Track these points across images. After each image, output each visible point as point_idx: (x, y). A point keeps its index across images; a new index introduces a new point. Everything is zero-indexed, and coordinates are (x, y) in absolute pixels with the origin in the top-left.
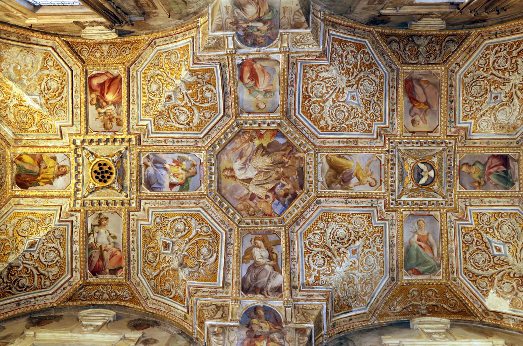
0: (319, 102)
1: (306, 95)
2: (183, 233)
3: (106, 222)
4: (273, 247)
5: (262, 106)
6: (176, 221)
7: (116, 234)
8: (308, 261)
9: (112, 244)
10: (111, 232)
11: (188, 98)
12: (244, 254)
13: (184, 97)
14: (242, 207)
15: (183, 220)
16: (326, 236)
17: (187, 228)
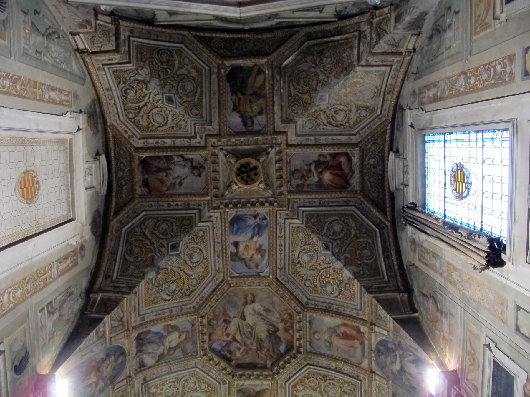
0: (320, 387)
1: (326, 377)
2: (189, 262)
3: (196, 174)
4: (180, 349)
5: (317, 336)
6: (201, 253)
7: (184, 185)
8: (170, 382)
9: (173, 181)
10: (186, 180)
11: (325, 268)
13: (326, 263)
14: (217, 314)
16: (193, 392)
17: (195, 265)
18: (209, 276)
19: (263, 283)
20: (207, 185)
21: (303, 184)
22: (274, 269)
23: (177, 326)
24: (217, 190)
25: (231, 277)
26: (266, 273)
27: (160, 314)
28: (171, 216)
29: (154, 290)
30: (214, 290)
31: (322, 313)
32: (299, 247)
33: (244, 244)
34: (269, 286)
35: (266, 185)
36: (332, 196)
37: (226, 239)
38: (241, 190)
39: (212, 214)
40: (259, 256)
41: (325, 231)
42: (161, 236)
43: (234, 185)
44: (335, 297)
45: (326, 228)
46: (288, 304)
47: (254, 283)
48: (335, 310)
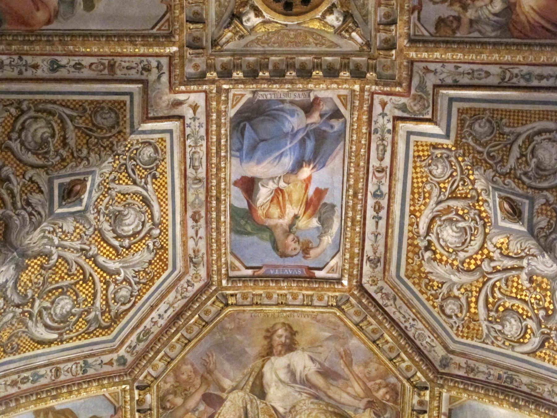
2: (110, 235)
6: (145, 208)
11: (505, 270)
12: (58, 408)
13: (508, 256)
14: (184, 377)
15: (148, 226)
17: (126, 243)
18: (164, 276)
19: (320, 299)
20: (169, 9)
21: (458, 19)
22: (356, 261)
23: (72, 413)
24: (200, 26)
25: (229, 278)
26: (332, 270)
27: (25, 380)
28: (60, 97)
29: (11, 315)
30: (178, 315)
31: (486, 395)
32: (432, 202)
33: (272, 186)
34: (338, 307)
35: (347, 16)
36: (543, 59)
37: (219, 169)
38: (270, 28)
39: (181, 97)
40: (315, 222)
41: (512, 162)
42: (31, 158)
43: (252, 15)
44: (528, 354)
45: (515, 152)
46: (391, 360)
47: (295, 298)
48: (524, 388)
